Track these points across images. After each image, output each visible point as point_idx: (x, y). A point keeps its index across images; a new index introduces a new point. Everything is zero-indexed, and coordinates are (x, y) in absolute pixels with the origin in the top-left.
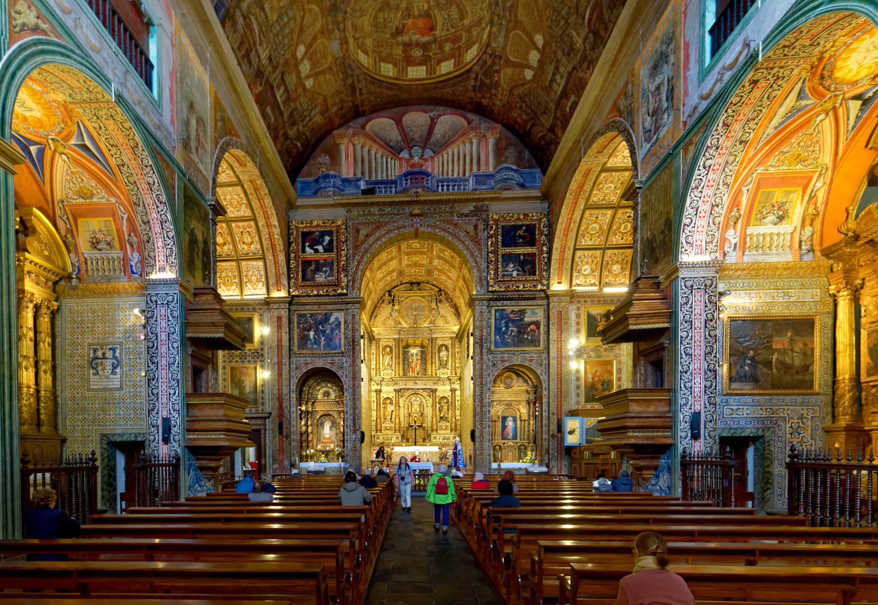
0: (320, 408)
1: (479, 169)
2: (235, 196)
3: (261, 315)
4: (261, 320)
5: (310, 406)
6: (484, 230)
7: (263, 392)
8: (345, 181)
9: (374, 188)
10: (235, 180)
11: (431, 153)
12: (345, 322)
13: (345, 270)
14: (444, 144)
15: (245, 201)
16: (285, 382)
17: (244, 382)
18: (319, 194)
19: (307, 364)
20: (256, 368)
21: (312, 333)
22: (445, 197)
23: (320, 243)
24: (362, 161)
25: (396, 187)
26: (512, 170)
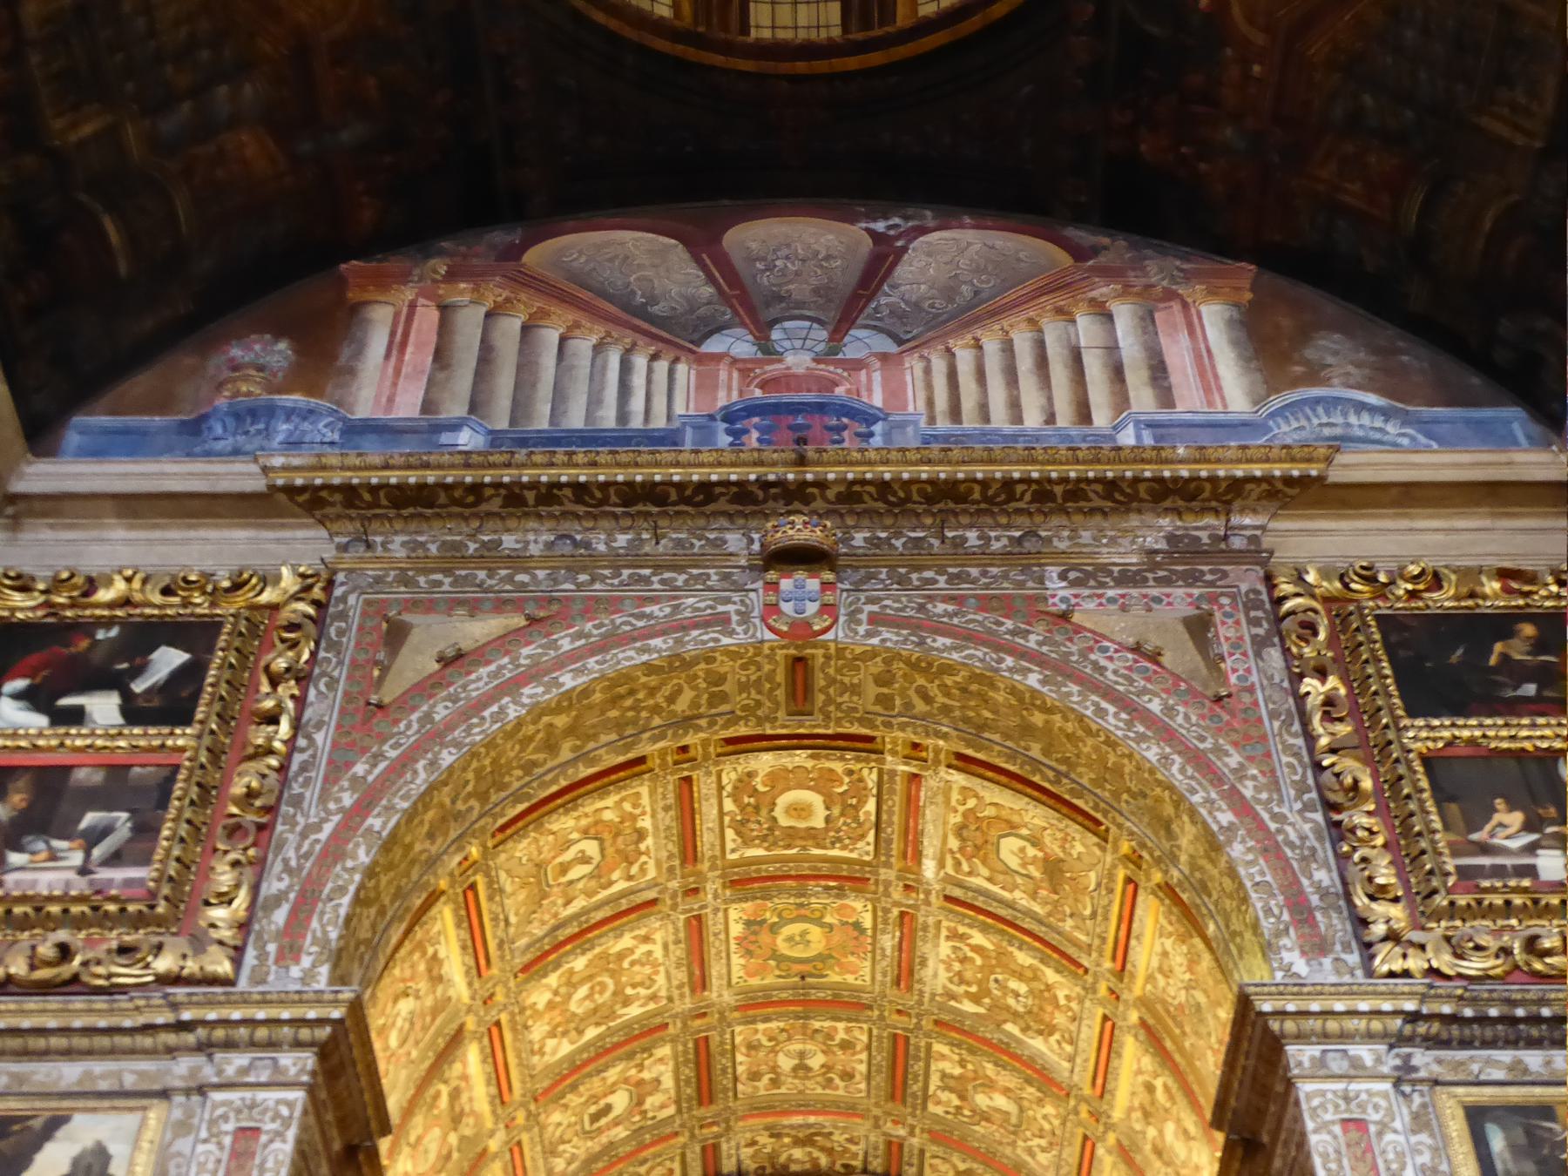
1: (1166, 397)
6: (1260, 644)
23: (117, 683)
26: (1361, 407)
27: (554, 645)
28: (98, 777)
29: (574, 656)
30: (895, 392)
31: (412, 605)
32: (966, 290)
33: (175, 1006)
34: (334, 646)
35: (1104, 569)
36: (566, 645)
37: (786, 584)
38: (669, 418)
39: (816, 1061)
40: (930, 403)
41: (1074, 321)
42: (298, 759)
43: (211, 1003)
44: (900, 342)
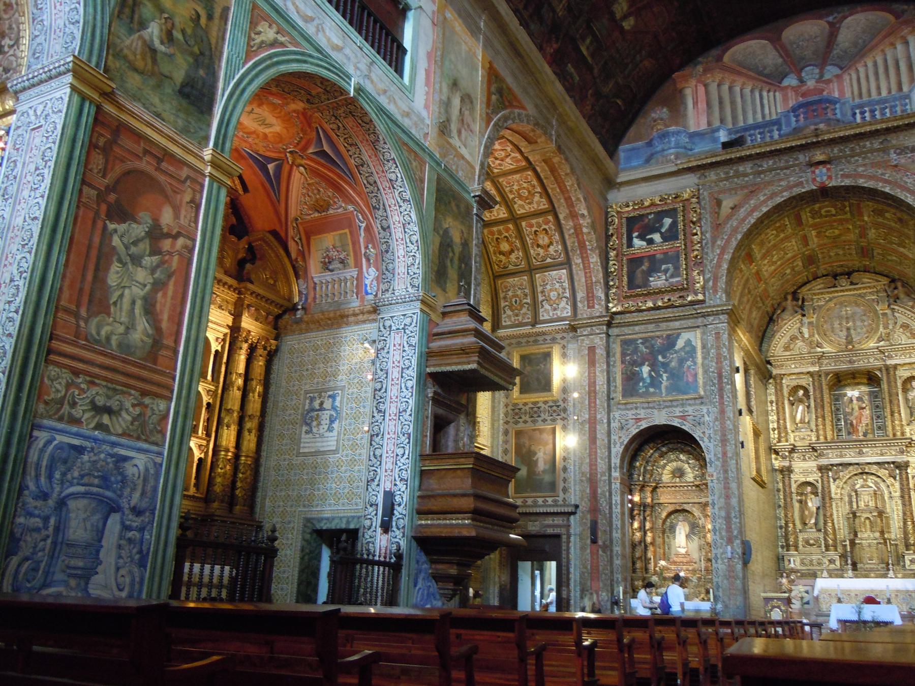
0: (667, 498)
2: (525, 185)
3: (564, 347)
4: (564, 355)
5: (649, 494)
7: (565, 469)
8: (692, 136)
9: (742, 137)
10: (524, 164)
11: (837, 71)
12: (704, 347)
13: (699, 263)
14: (860, 52)
15: (539, 189)
16: (601, 452)
17: (535, 454)
18: (653, 161)
19: (639, 420)
20: (554, 431)
21: (646, 369)
22: (868, 129)
23: (658, 230)
24: (721, 103)
25: (779, 130)
27: (758, 199)
28: (662, 256)
29: (764, 202)
30: (842, 92)
31: (720, 192)
32: (860, 41)
33: (695, 309)
34: (704, 208)
35: (907, 148)
36: (762, 198)
37: (817, 171)
38: (777, 114)
39: (841, 252)
40: (853, 93)
41: (895, 48)
42: (704, 242)
43: (703, 308)
44: (841, 68)
